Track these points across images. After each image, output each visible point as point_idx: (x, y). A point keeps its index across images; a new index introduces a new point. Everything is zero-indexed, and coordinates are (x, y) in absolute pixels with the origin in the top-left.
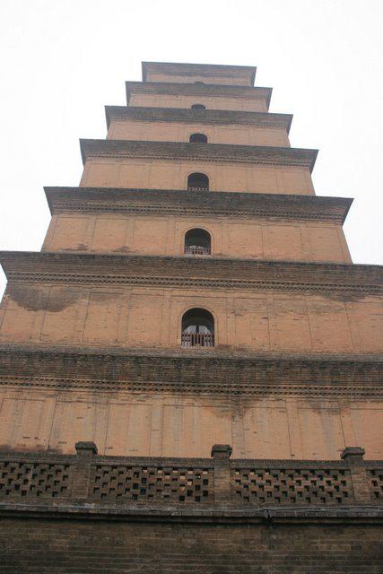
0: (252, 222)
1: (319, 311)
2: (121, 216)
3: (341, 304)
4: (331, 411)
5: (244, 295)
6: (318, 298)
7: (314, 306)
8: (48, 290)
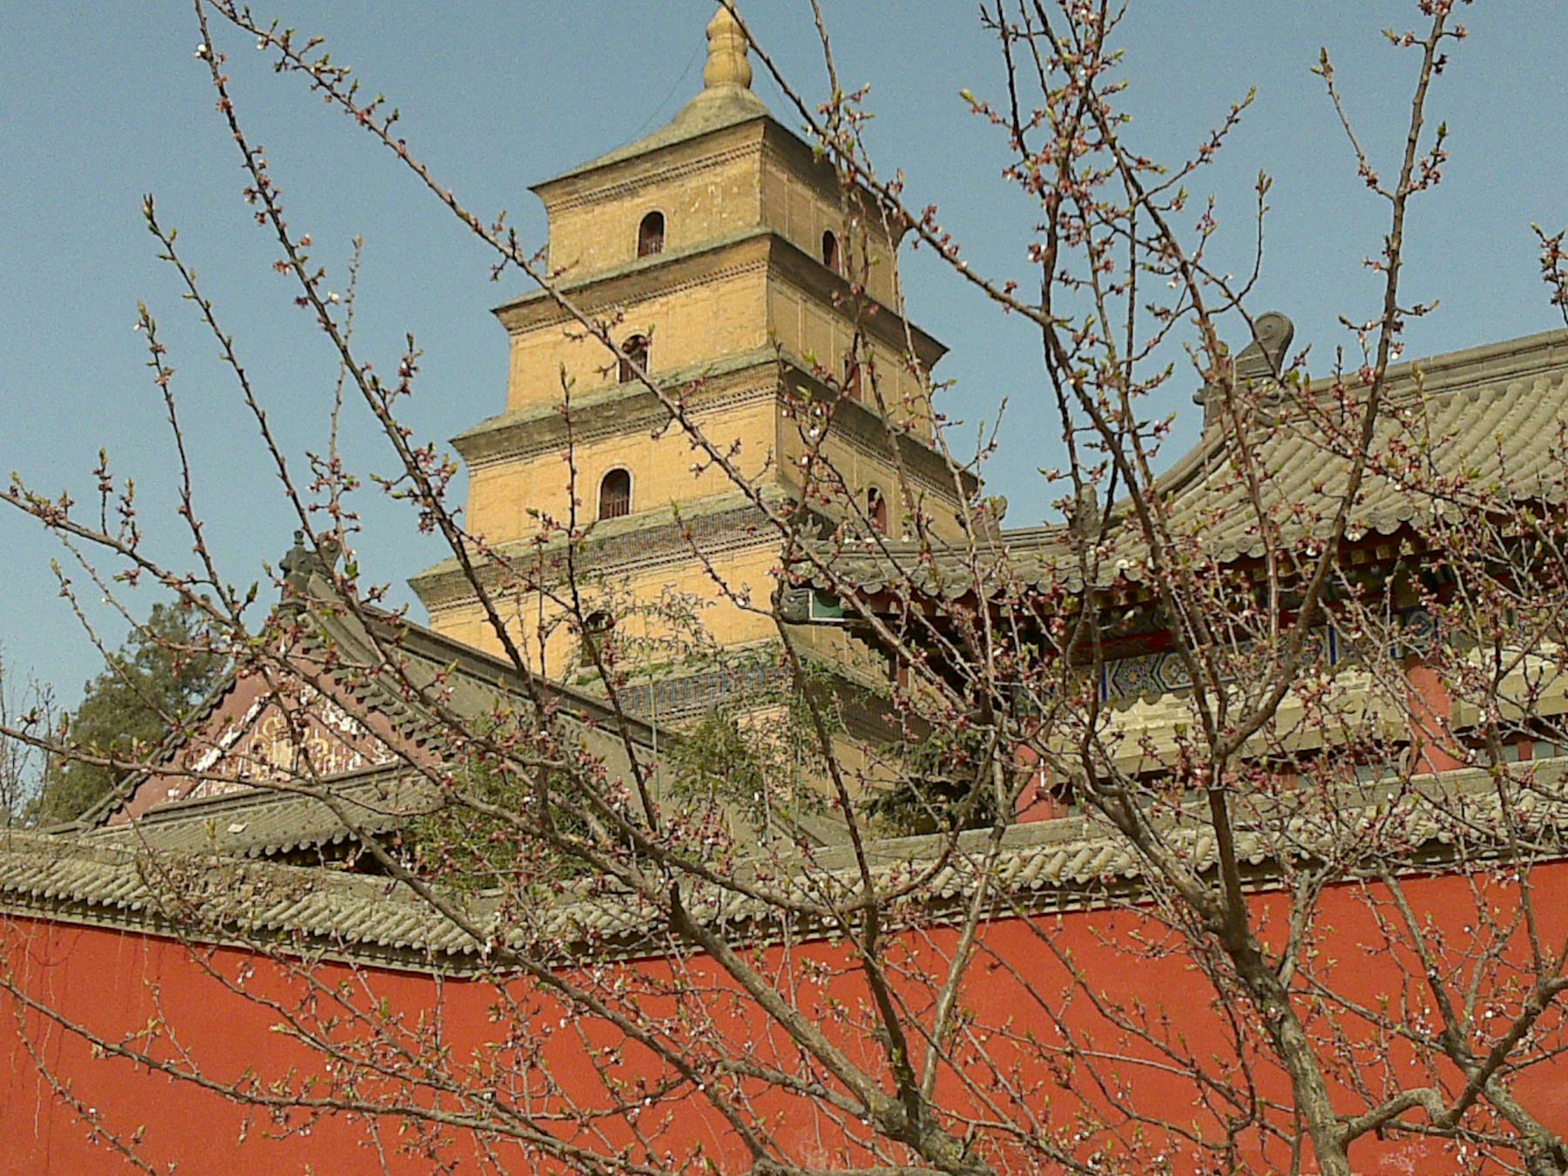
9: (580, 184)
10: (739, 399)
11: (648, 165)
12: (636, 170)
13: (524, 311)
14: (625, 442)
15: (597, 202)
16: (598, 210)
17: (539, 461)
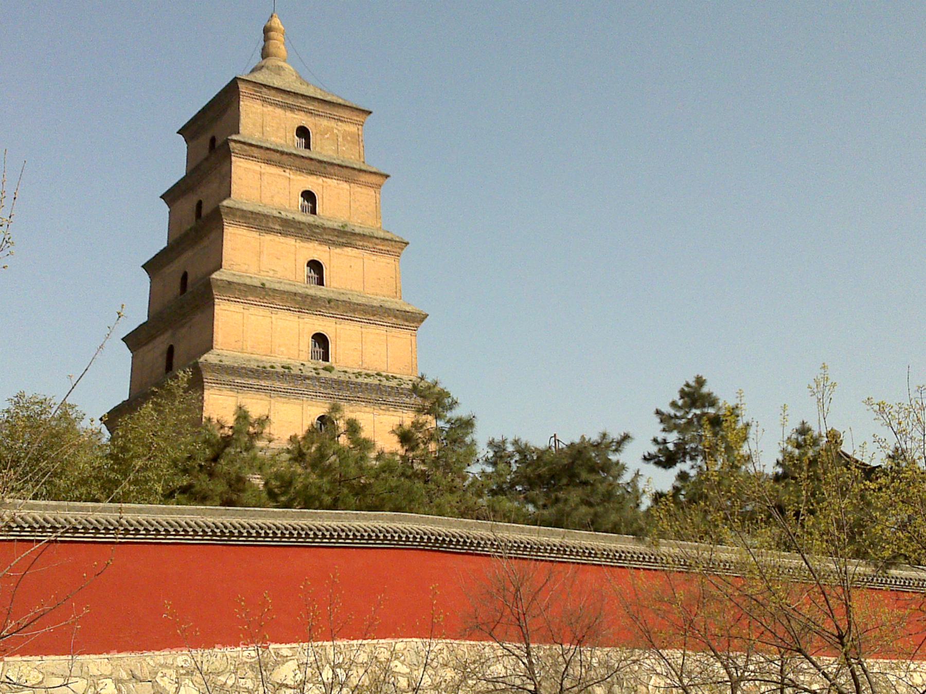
0: (367, 409)
2: (263, 396)
10: (381, 251)
11: (304, 101)
12: (296, 100)
13: (246, 147)
14: (320, 247)
15: (271, 104)
16: (270, 108)
17: (268, 237)
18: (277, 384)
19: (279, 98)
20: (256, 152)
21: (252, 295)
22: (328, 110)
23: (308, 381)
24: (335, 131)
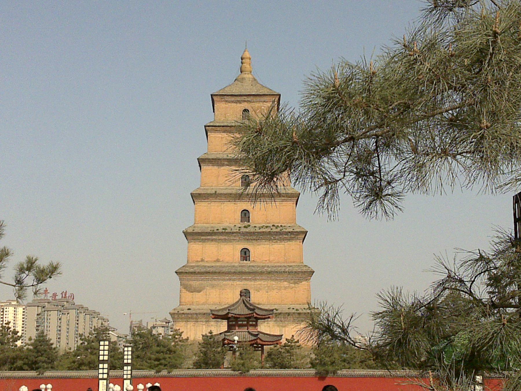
0: (266, 243)
1: (286, 288)
3: (293, 285)
4: (283, 327)
5: (260, 283)
6: (286, 283)
7: (284, 287)
8: (195, 283)
9: (225, 97)
13: (213, 128)
15: (229, 102)
16: (229, 104)
17: (223, 168)
18: (221, 237)
19: (233, 99)
20: (218, 129)
21: (211, 197)
22: (258, 98)
23: (235, 234)
24: (263, 107)
